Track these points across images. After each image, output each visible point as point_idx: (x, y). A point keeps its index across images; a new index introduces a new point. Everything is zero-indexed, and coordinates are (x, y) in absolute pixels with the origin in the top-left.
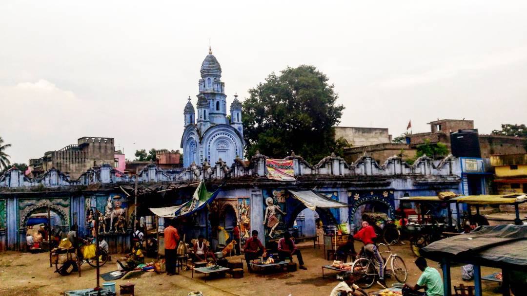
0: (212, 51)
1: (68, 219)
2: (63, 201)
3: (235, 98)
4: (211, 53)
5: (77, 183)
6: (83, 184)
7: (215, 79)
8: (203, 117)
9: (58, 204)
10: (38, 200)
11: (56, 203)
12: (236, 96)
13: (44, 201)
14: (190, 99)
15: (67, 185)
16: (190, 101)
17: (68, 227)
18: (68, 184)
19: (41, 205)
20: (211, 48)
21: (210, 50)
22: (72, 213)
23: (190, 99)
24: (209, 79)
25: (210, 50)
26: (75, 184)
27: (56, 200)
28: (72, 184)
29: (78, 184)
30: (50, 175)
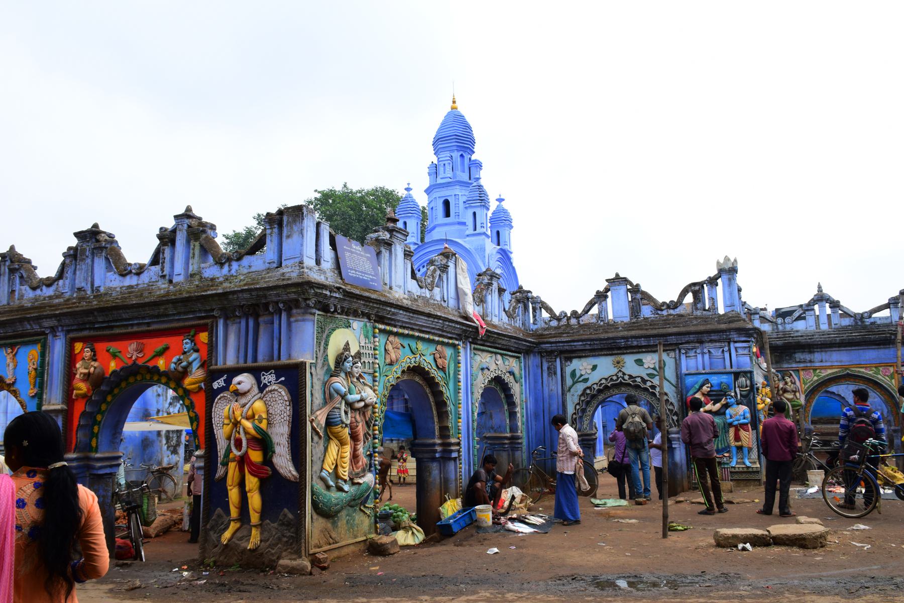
0: (457, 104)
3: (498, 203)
4: (457, 109)
12: (500, 200)
16: (411, 192)
20: (456, 100)
21: (454, 102)
25: (454, 102)
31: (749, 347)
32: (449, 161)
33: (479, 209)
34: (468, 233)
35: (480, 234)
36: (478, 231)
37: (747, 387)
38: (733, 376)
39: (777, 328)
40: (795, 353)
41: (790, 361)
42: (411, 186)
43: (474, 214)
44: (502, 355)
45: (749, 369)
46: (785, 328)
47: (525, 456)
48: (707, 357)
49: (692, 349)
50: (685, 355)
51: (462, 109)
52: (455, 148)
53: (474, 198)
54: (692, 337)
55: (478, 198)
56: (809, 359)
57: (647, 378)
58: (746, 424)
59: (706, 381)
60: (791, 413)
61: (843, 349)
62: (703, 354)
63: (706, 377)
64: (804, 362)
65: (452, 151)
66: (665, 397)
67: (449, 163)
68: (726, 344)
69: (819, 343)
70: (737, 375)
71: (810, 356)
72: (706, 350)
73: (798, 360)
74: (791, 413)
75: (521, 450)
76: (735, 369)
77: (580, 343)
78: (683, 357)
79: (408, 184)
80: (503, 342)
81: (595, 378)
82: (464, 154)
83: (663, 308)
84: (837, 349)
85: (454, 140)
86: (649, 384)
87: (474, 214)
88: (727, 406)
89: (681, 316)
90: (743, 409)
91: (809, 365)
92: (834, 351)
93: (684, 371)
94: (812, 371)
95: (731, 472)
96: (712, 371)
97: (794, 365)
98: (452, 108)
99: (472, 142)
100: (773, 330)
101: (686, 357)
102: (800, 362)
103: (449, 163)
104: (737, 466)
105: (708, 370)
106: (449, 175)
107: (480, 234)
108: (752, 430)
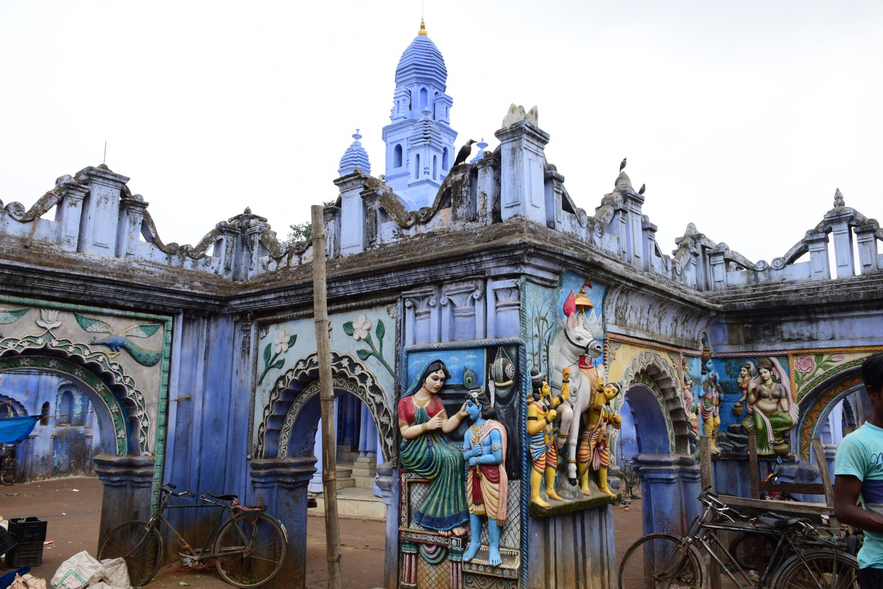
1: (153, 429)
2: (141, 333)
5: (195, 265)
6: (221, 271)
7: (436, 93)
8: (431, 171)
9: (113, 346)
10: (21, 309)
11: (101, 338)
13: (52, 318)
14: (357, 136)
15: (155, 264)
16: (360, 140)
17: (150, 465)
18: (160, 257)
19: (31, 339)
21: (423, 27)
22: (173, 396)
23: (357, 136)
24: (424, 90)
25: (423, 27)
26: (188, 264)
27: (110, 321)
28: (175, 260)
29: (200, 268)
30: (87, 198)
31: (517, 288)
32: (404, 97)
33: (423, 149)
34: (410, 182)
35: (422, 182)
36: (420, 179)
37: (506, 379)
38: (484, 355)
39: (756, 279)
40: (781, 323)
41: (773, 339)
42: (360, 133)
43: (418, 156)
44: (74, 311)
45: (515, 338)
46: (770, 277)
47: (154, 500)
48: (446, 312)
49: (423, 298)
50: (412, 310)
51: (432, 36)
52: (414, 81)
53: (417, 137)
54: (421, 274)
55: (423, 136)
56: (807, 334)
57: (357, 359)
58: (495, 465)
59: (438, 365)
60: (771, 438)
61: (876, 312)
62: (441, 307)
63: (434, 356)
64: (799, 340)
65: (412, 85)
66: (378, 399)
67: (404, 100)
68: (480, 284)
69: (824, 301)
70: (492, 351)
71: (809, 327)
72: (444, 300)
73: (786, 336)
74: (771, 438)
75: (150, 487)
76: (491, 340)
77: (273, 296)
78: (410, 314)
79: (358, 130)
80: (62, 287)
81: (292, 358)
82: (427, 88)
83: (409, 223)
84: (863, 313)
85: (413, 71)
86: (358, 371)
87: (418, 156)
88: (468, 421)
89: (432, 235)
90: (496, 427)
91: (806, 345)
92: (858, 317)
93: (409, 345)
94: (813, 358)
95: (463, 573)
96: (454, 344)
97: (778, 346)
98: (421, 34)
99: (444, 73)
100: (749, 282)
101: (416, 315)
102: (790, 340)
103: (404, 100)
104: (475, 561)
105: (446, 343)
106: (403, 115)
107: (422, 182)
108: (510, 478)
